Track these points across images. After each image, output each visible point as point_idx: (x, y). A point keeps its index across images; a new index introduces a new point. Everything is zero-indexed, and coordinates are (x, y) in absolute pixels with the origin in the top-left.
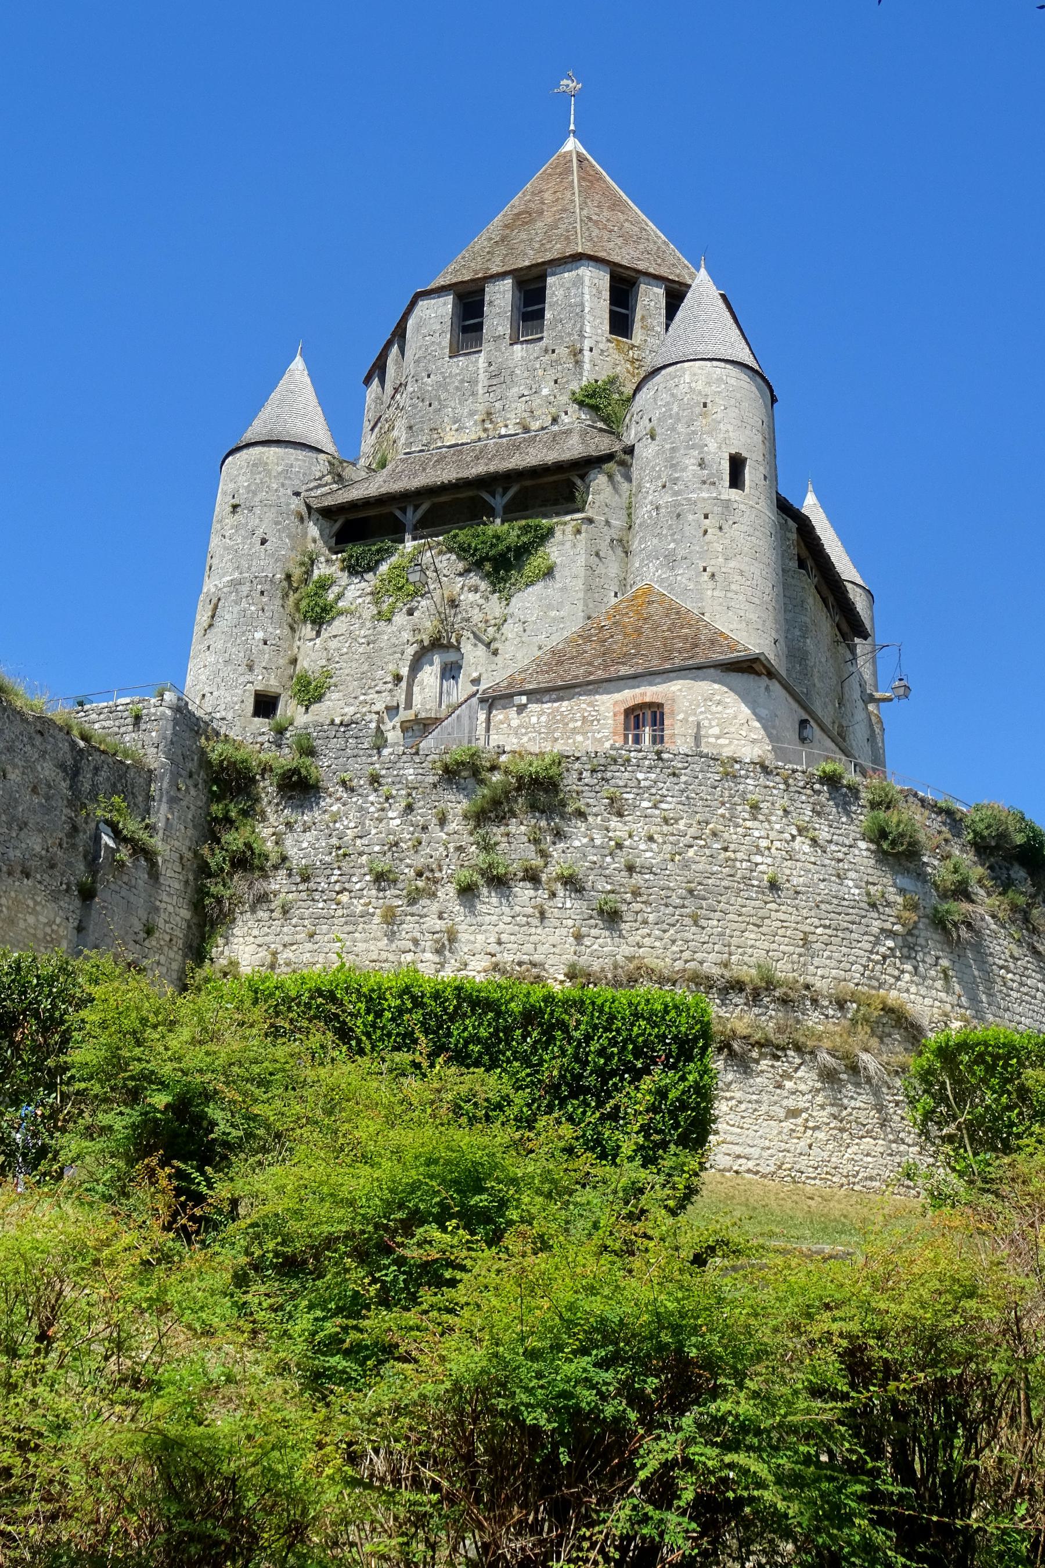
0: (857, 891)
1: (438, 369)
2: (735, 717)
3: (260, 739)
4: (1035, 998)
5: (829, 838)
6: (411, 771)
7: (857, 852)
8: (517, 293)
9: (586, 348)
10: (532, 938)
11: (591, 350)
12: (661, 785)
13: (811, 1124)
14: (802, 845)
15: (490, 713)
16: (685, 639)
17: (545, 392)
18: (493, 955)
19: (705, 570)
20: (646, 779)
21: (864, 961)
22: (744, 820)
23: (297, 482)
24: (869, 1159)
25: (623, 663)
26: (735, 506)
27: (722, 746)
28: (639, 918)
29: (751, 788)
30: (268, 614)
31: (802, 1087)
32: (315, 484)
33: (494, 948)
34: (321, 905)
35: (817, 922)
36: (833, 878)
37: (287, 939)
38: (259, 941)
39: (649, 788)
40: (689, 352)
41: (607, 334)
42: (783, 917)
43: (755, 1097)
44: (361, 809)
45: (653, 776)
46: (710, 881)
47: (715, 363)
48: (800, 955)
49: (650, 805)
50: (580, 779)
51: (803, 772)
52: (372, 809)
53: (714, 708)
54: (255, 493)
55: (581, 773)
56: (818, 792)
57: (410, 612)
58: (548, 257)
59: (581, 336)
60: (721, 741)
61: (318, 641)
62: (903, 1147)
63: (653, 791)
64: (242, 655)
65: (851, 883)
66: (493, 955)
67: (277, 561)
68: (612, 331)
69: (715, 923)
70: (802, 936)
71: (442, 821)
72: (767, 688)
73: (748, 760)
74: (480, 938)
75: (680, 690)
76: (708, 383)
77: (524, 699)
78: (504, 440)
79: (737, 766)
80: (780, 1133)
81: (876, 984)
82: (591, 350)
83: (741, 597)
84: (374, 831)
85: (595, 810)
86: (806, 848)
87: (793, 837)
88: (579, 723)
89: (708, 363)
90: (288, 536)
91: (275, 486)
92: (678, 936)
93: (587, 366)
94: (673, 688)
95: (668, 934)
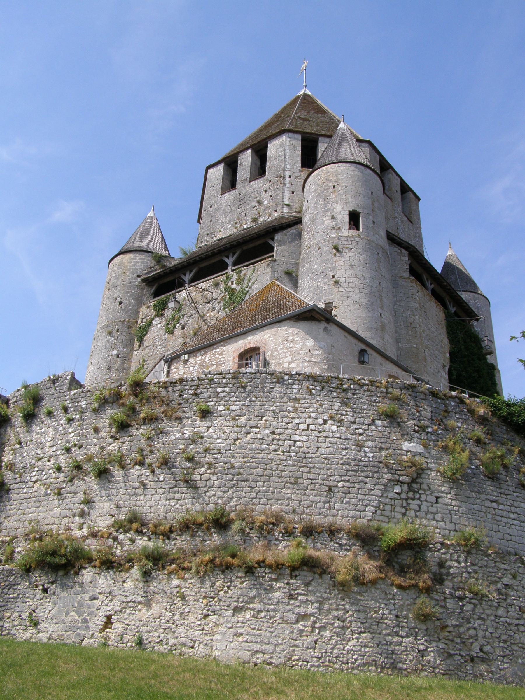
0: (372, 455)
1: (215, 202)
3: (17, 394)
6: (85, 402)
8: (256, 158)
12: (232, 394)
13: (318, 625)
14: (332, 427)
15: (169, 367)
17: (266, 202)
20: (224, 391)
21: (375, 503)
22: (289, 412)
27: (292, 368)
33: (114, 511)
34: (25, 491)
35: (338, 478)
36: (353, 447)
39: (225, 396)
40: (327, 161)
41: (300, 168)
42: (311, 476)
43: (272, 607)
44: (55, 429)
45: (227, 389)
46: (261, 456)
48: (325, 502)
49: (224, 408)
50: (180, 396)
52: (61, 428)
53: (288, 345)
54: (118, 279)
55: (182, 392)
59: (284, 171)
60: (293, 365)
63: (227, 399)
64: (105, 364)
65: (367, 449)
67: (126, 312)
72: (325, 329)
75: (269, 337)
77: (186, 356)
79: (286, 377)
80: (292, 632)
82: (290, 177)
83: (357, 291)
84: (60, 442)
85: (187, 415)
86: (334, 428)
87: (325, 422)
89: (336, 165)
90: (133, 299)
92: (234, 495)
93: (288, 185)
94: (265, 337)
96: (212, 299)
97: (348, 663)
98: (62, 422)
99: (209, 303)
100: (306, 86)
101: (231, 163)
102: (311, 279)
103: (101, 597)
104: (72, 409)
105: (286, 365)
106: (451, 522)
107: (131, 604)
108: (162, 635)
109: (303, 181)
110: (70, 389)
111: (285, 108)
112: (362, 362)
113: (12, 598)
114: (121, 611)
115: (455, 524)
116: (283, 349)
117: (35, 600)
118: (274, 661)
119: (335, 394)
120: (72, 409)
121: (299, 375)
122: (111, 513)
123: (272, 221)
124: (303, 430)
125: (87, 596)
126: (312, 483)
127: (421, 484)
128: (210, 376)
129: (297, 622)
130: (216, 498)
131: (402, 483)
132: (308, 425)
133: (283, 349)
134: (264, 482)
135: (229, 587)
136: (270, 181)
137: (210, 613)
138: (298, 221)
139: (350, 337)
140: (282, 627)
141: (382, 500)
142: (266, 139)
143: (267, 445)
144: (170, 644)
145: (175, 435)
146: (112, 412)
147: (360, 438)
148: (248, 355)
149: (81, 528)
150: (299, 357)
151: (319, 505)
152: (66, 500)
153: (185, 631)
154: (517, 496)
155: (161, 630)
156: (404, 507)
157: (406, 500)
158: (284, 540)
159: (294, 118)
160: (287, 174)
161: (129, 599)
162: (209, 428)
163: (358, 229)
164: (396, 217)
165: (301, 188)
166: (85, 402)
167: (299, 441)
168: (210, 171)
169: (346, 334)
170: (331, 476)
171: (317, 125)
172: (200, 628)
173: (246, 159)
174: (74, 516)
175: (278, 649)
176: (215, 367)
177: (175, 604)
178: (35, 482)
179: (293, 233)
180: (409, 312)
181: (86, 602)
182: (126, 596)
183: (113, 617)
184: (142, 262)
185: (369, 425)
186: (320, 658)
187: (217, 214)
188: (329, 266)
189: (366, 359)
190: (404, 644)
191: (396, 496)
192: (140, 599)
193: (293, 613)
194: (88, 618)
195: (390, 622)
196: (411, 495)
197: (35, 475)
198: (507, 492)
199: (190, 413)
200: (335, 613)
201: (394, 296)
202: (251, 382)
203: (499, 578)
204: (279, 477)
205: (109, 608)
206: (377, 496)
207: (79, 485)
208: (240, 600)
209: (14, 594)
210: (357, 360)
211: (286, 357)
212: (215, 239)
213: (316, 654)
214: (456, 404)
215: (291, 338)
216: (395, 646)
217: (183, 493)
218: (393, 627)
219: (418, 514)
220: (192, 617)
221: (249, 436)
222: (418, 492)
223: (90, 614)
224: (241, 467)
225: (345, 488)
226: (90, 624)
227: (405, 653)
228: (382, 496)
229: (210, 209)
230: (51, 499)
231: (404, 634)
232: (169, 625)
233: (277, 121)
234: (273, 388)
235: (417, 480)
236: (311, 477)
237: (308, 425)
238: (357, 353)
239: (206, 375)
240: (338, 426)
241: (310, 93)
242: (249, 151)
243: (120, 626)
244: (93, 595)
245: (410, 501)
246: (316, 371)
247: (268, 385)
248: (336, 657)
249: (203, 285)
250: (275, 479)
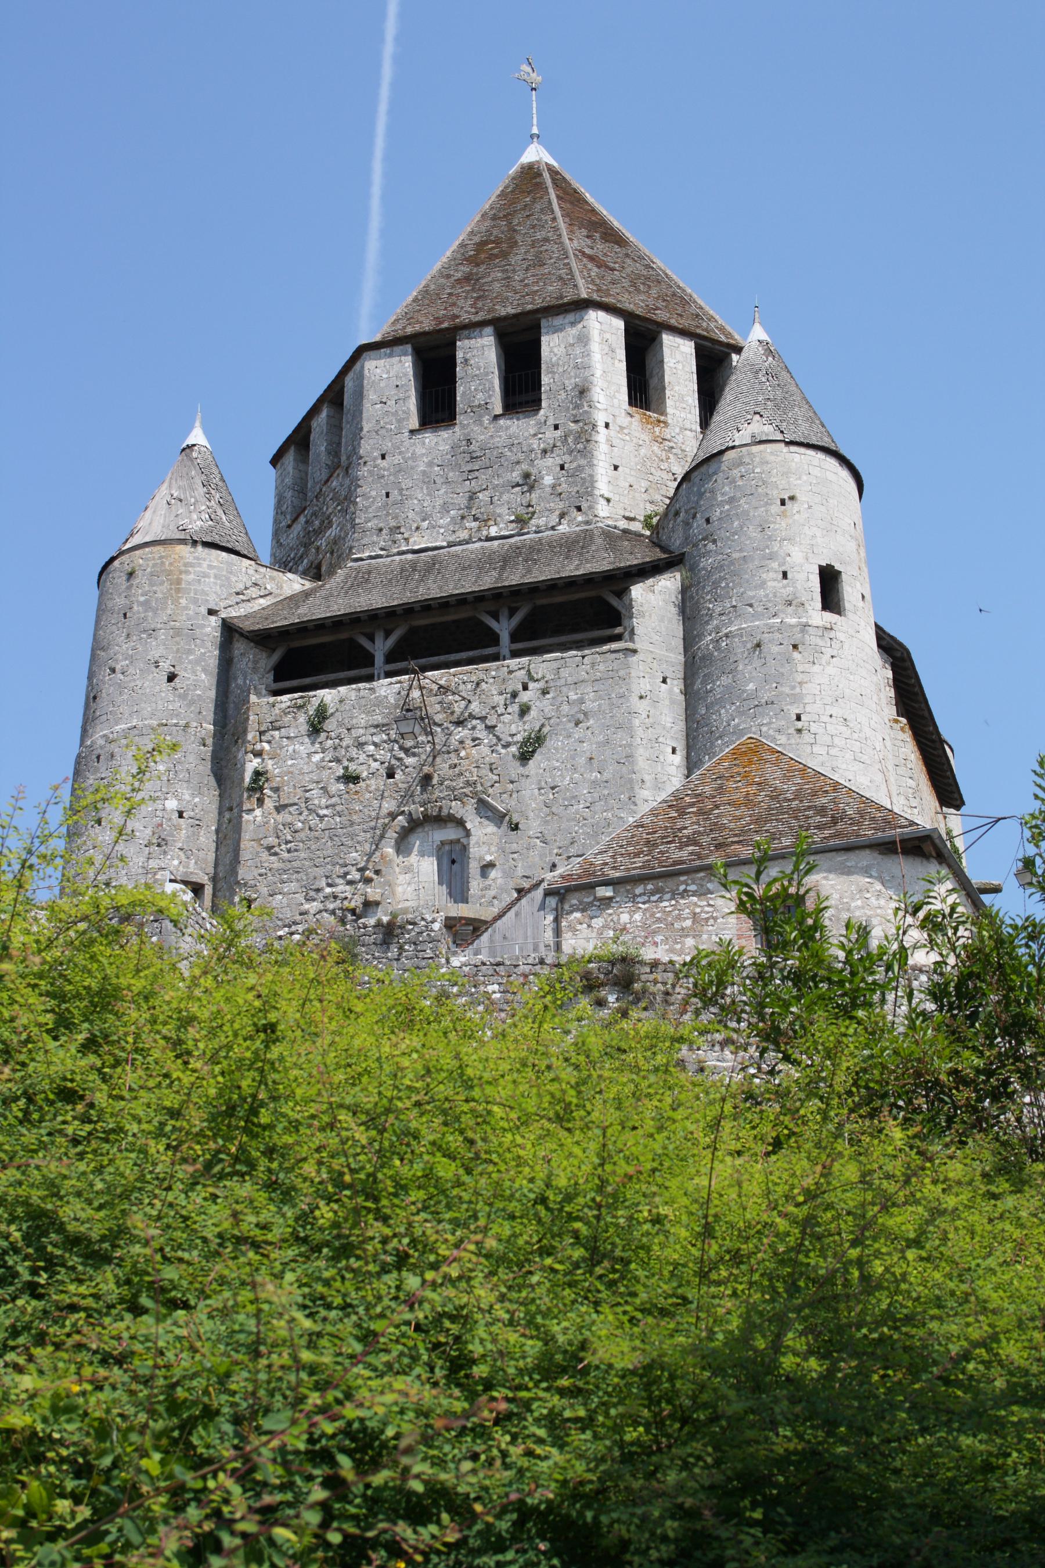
9: (601, 424)
11: (607, 425)
16: (822, 811)
17: (548, 480)
47: (793, 448)
57: (391, 775)
58: (539, 303)
68: (630, 404)
78: (496, 543)
82: (607, 425)
88: (688, 923)
90: (204, 670)
99: (459, 723)
136: (556, 427)
160: (600, 418)
184: (216, 577)
229: (383, 464)
241: (555, 164)
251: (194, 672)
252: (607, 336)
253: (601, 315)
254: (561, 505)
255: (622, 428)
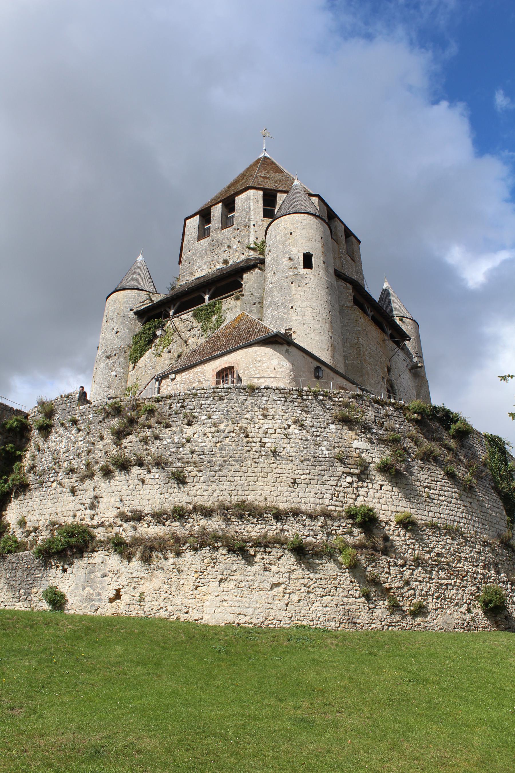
0: (327, 452)
2: (268, 368)
3: (34, 410)
4: (451, 502)
5: (311, 425)
7: (329, 431)
10: (139, 497)
11: (254, 225)
12: (212, 406)
13: (288, 591)
14: (294, 430)
15: (160, 385)
17: (235, 247)
18: (118, 508)
19: (292, 307)
20: (206, 404)
21: (331, 492)
22: (259, 419)
23: (131, 305)
24: (328, 609)
25: (218, 350)
26: (307, 276)
27: (260, 383)
28: (195, 480)
29: (264, 402)
30: (118, 363)
31: (282, 569)
32: (141, 304)
33: (119, 504)
36: (312, 446)
37: (29, 509)
38: (19, 511)
41: (262, 218)
43: (251, 578)
45: (208, 402)
46: (237, 455)
47: (295, 215)
49: (206, 417)
50: (170, 408)
51: (296, 390)
53: (257, 365)
54: (114, 313)
55: (171, 405)
56: (305, 400)
59: (249, 220)
60: (262, 381)
61: (133, 372)
62: (351, 600)
63: (209, 410)
64: (106, 383)
65: (324, 448)
66: (118, 508)
67: (122, 340)
68: (264, 217)
69: (239, 478)
70: (292, 481)
71: (102, 438)
72: (287, 351)
73: (263, 387)
74: (113, 499)
76: (293, 224)
77: (174, 375)
81: (341, 504)
82: (254, 225)
83: (311, 318)
84: (72, 449)
86: (297, 431)
87: (289, 426)
91: (122, 308)
92: (217, 488)
93: (252, 233)
94: (238, 358)
95: (211, 487)
96: (193, 328)
97: (313, 621)
98: (73, 432)
100: (265, 150)
101: (205, 215)
102: (273, 310)
103: (111, 575)
104: (81, 421)
105: (256, 381)
106: (393, 505)
107: (135, 579)
108: (162, 604)
109: (265, 229)
110: (78, 405)
111: (248, 168)
112: (317, 377)
113: (38, 577)
114: (128, 585)
115: (396, 506)
116: (253, 367)
117: (57, 579)
118: (253, 621)
119: (296, 404)
120: (81, 421)
121: (267, 389)
122: (116, 506)
123: (240, 262)
124: (272, 434)
125: (99, 574)
126: (280, 477)
127: (368, 475)
128: (194, 391)
129: (271, 588)
130: (202, 491)
131: (352, 474)
132: (275, 430)
133: (253, 367)
134: (241, 477)
135: (215, 563)
136: (238, 229)
137: (200, 584)
138: (262, 262)
139: (307, 357)
140: (259, 594)
141: (337, 488)
142: (233, 194)
143: (243, 446)
144: (169, 611)
145: (167, 441)
146: (115, 423)
147: (318, 438)
148: (224, 374)
149: (92, 519)
150: (266, 375)
151: (287, 494)
152: (78, 496)
153: (181, 600)
154: (445, 482)
155: (162, 600)
156: (355, 494)
157: (357, 488)
158: (259, 524)
159: (256, 177)
160: (252, 224)
161: (133, 576)
162: (194, 434)
163: (311, 268)
164: (341, 258)
165: (264, 235)
166: (91, 416)
167: (269, 442)
168: (188, 221)
169: (304, 355)
170: (295, 470)
171: (276, 182)
172: (193, 597)
173: (217, 211)
174: (86, 509)
175: (257, 612)
176: (197, 383)
177: (172, 578)
178: (52, 482)
179: (258, 272)
180: (354, 335)
181: (99, 579)
182: (131, 573)
183: (121, 590)
184: (133, 298)
185: (324, 428)
186: (291, 618)
187: (195, 258)
188: (288, 298)
189: (320, 375)
190: (358, 604)
191: (348, 485)
192: (142, 575)
193: (268, 582)
194: (101, 592)
195: (346, 587)
196: (360, 484)
197: (52, 477)
198: (436, 479)
199: (179, 422)
200: (301, 581)
201: (342, 323)
202: (227, 395)
203: (431, 548)
204: (253, 472)
205: (117, 583)
206: (333, 486)
207: (89, 484)
208: (225, 573)
209: (39, 574)
210: (313, 375)
211: (256, 374)
212: (194, 278)
213: (287, 615)
214: (394, 409)
215: (259, 359)
216: (350, 605)
217: (175, 488)
218: (349, 591)
219: (366, 499)
220: (186, 589)
221: (227, 439)
222: (365, 481)
223: (103, 588)
224: (220, 465)
225: (307, 480)
226: (103, 597)
227: (358, 611)
228: (337, 486)
230: (66, 495)
231: (357, 596)
232: (167, 595)
233: (243, 179)
234: (246, 400)
235: (365, 472)
236: (279, 472)
237: (275, 430)
238: (313, 370)
239: (191, 390)
240: (301, 430)
241: (269, 156)
242: (220, 204)
243: (128, 597)
244: (104, 573)
245: (359, 489)
246: (281, 385)
247: (242, 397)
248: (304, 616)
249: (185, 317)
250: (249, 474)
251: (124, 330)
252: (256, 197)
253: (254, 191)
254: (238, 254)
255: (260, 226)
